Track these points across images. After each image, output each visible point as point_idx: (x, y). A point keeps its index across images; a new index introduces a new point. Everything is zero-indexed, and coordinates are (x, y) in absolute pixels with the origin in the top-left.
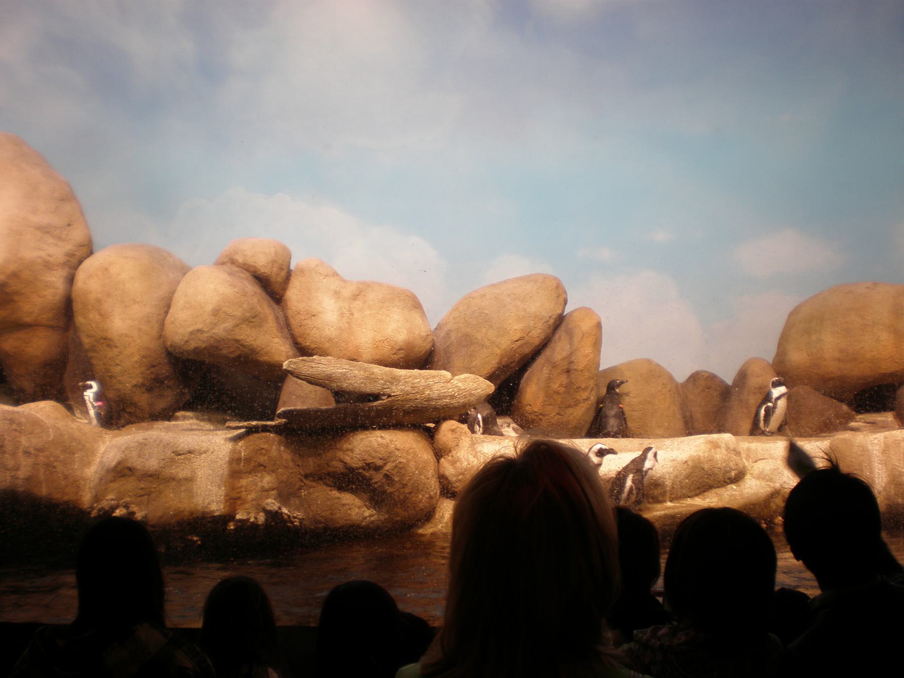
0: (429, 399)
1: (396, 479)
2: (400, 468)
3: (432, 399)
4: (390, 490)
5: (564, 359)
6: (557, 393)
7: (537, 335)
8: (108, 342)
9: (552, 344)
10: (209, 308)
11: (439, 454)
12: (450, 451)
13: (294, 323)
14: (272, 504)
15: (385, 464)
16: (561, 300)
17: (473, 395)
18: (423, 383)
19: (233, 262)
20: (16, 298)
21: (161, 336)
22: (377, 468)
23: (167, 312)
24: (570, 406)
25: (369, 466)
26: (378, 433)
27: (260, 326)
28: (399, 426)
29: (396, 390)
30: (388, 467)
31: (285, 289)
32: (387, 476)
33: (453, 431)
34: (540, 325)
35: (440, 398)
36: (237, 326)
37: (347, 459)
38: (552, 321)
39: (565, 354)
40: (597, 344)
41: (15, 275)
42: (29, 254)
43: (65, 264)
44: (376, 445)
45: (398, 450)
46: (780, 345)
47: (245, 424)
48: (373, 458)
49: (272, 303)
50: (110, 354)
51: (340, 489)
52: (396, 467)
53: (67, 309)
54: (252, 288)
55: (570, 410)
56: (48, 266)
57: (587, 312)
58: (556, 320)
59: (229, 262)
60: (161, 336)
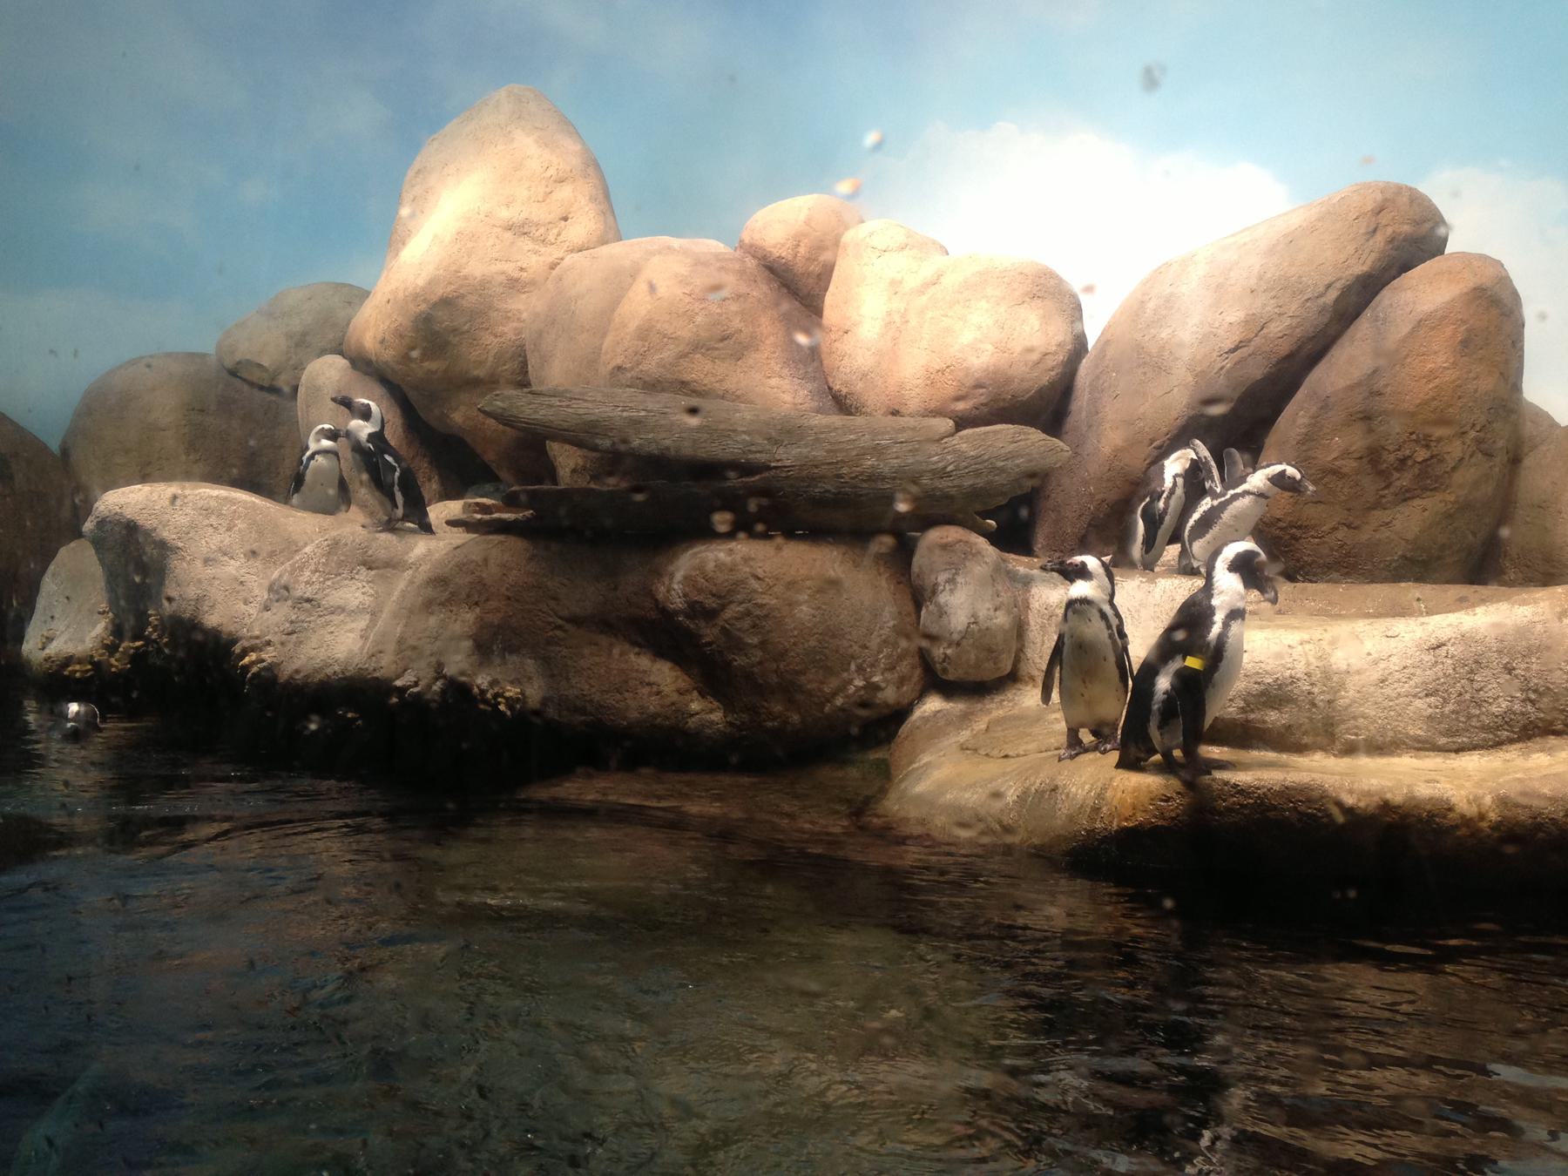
2: (759, 619)
3: (884, 479)
4: (740, 661)
5: (1351, 388)
6: (1335, 472)
12: (934, 592)
14: (458, 662)
15: (723, 607)
17: (1002, 470)
18: (866, 441)
22: (711, 615)
25: (697, 611)
28: (816, 533)
33: (945, 547)
44: (711, 566)
45: (758, 578)
48: (700, 591)
52: (748, 613)
58: (1346, 292)
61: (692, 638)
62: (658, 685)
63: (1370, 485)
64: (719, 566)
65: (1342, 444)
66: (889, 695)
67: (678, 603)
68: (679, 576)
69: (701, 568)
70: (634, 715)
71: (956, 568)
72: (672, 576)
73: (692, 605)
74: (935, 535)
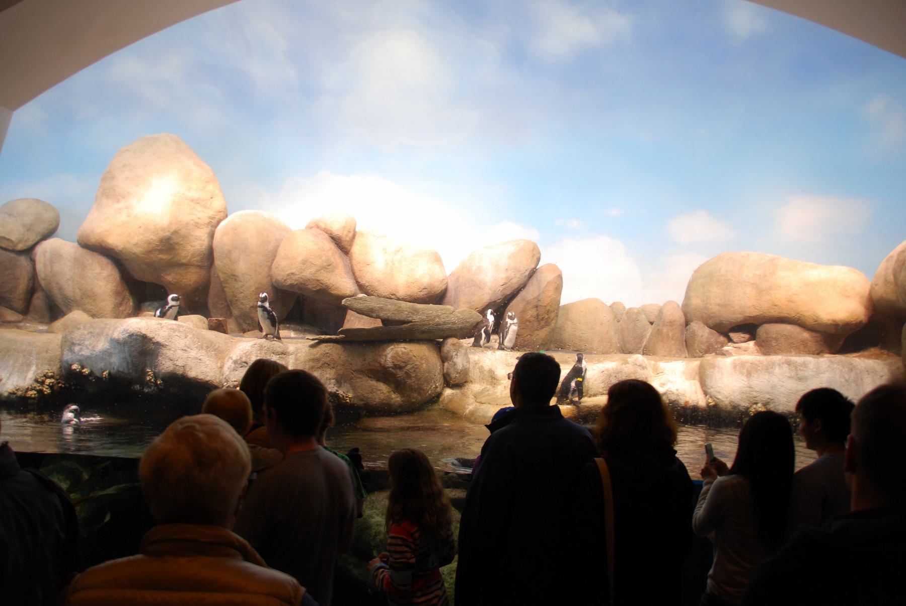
0: (438, 324)
1: (413, 375)
2: (416, 369)
4: (409, 381)
6: (530, 321)
7: (516, 281)
8: (234, 277)
9: (527, 287)
10: (300, 259)
11: (444, 359)
13: (356, 268)
16: (535, 259)
19: (318, 227)
20: (177, 247)
21: (270, 276)
22: (401, 368)
23: (273, 260)
24: (537, 330)
25: (396, 367)
26: (403, 345)
27: (333, 271)
29: (416, 318)
30: (408, 367)
31: (351, 245)
32: (406, 373)
33: (454, 345)
34: (518, 276)
35: (445, 323)
36: (318, 271)
37: (382, 361)
38: (527, 273)
39: (535, 295)
40: (558, 288)
41: (176, 232)
42: (185, 218)
43: (208, 224)
46: (687, 293)
47: (318, 337)
49: (342, 254)
50: (237, 286)
51: (378, 380)
53: (210, 255)
54: (330, 246)
55: (537, 332)
56: (197, 225)
57: (553, 268)
59: (315, 226)
60: (270, 276)
61: (393, 375)
62: (382, 392)
63: (536, 324)
64: (403, 353)
65: (531, 313)
66: (439, 390)
67: (390, 365)
68: (389, 356)
69: (397, 353)
70: (377, 400)
71: (457, 350)
72: (386, 356)
73: (395, 365)
74: (450, 341)
